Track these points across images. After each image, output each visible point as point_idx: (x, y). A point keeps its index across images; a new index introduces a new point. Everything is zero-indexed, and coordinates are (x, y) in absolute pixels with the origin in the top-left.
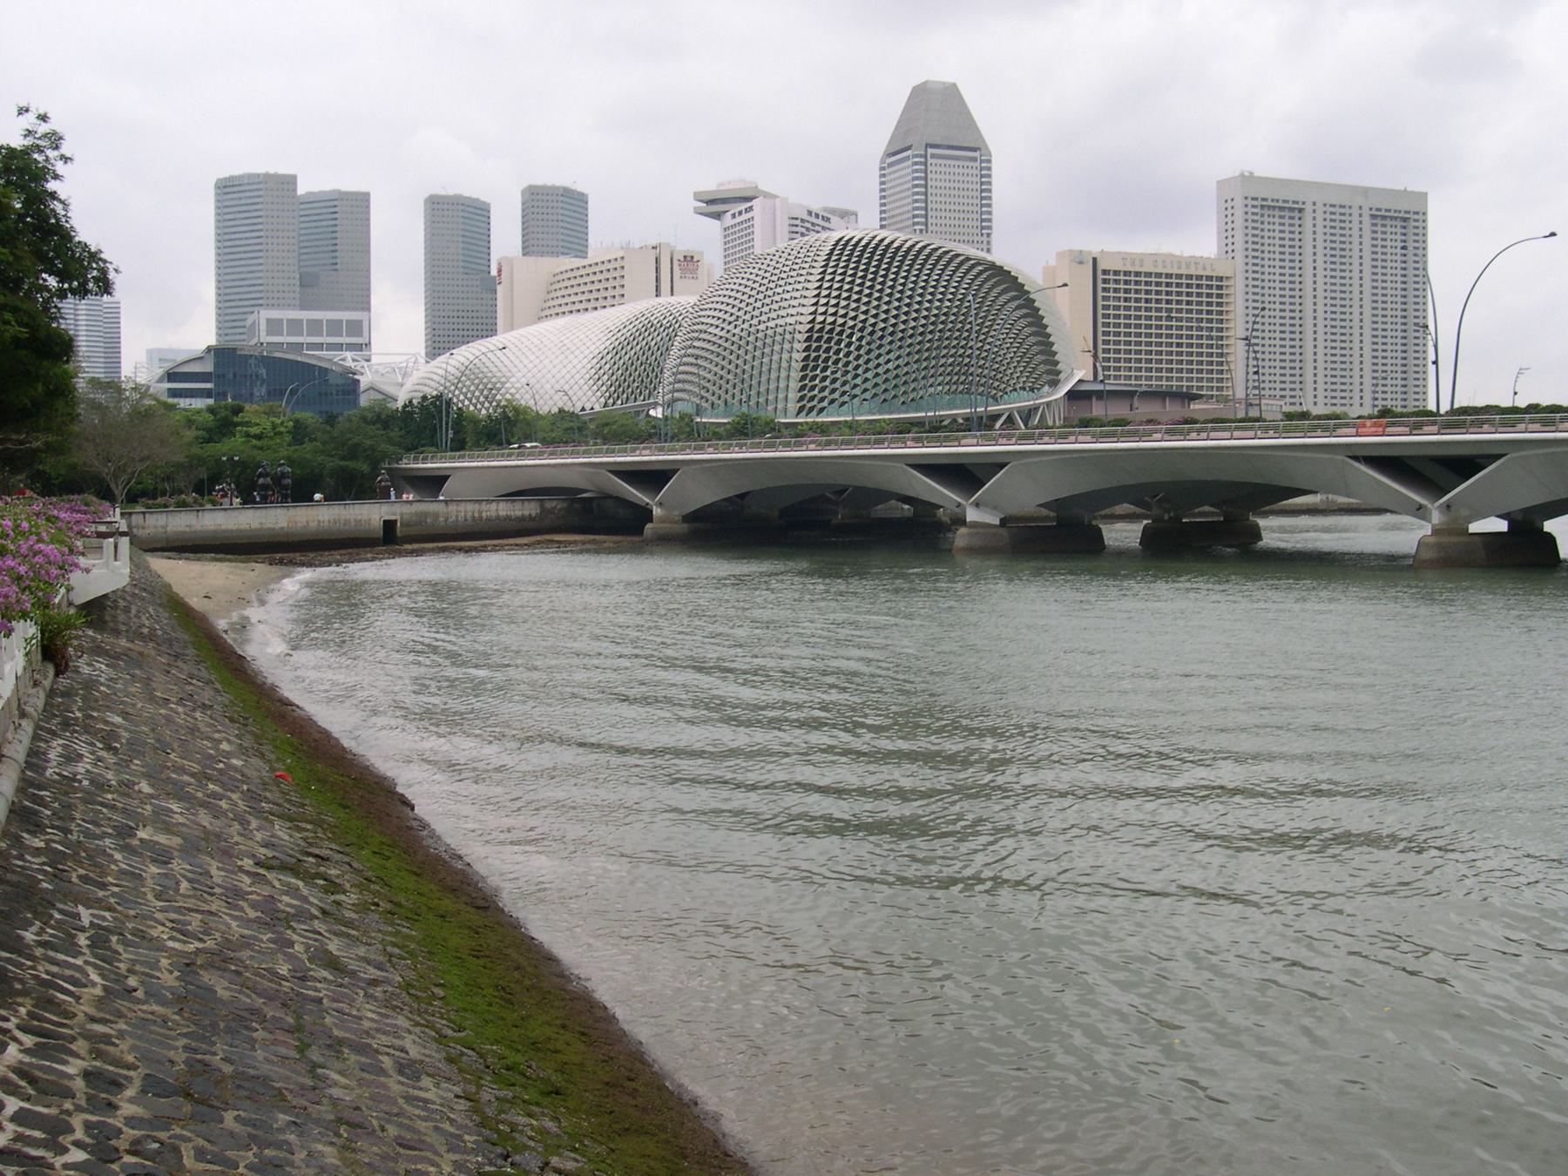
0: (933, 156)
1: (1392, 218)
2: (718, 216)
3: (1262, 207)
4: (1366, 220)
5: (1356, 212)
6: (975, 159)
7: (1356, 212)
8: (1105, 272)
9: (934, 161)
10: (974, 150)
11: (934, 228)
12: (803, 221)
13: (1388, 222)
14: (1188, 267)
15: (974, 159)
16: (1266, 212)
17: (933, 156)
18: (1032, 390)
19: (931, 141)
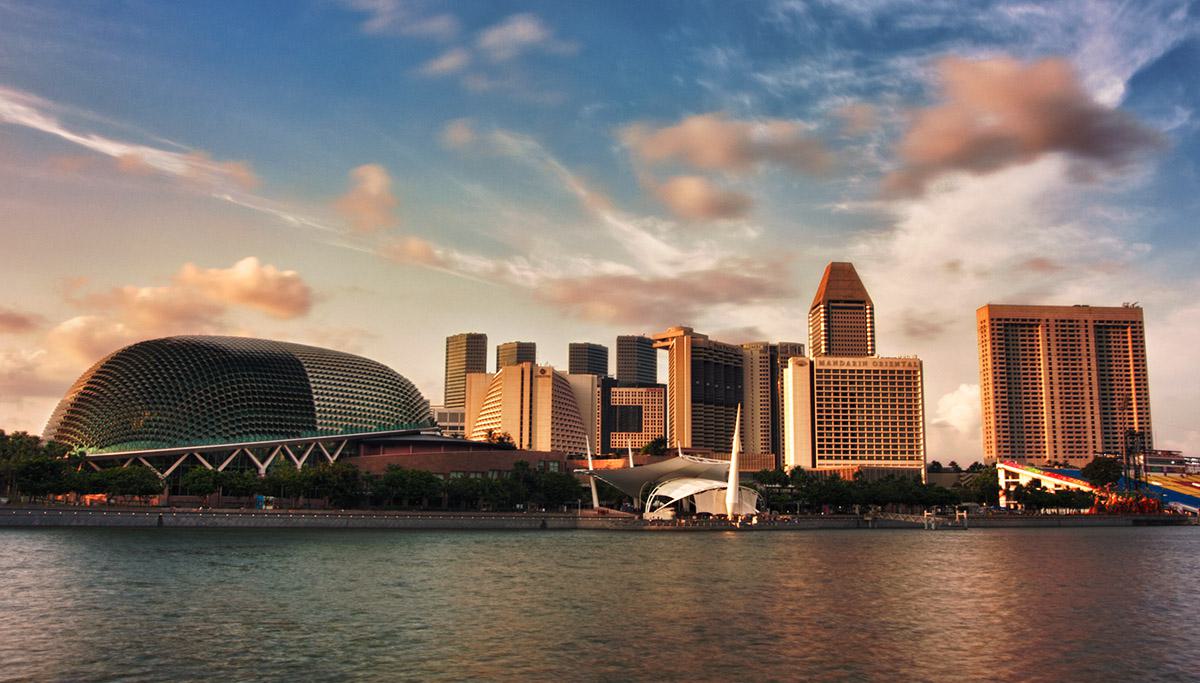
0: (833, 307)
1: (1114, 327)
2: (666, 348)
3: (1006, 325)
4: (1091, 329)
5: (1082, 324)
6: (862, 308)
7: (1082, 324)
8: (818, 371)
9: (834, 311)
10: (861, 302)
11: (835, 352)
12: (705, 349)
13: (1111, 330)
14: (891, 366)
15: (862, 308)
16: (1010, 328)
17: (833, 307)
18: (227, 438)
19: (832, 298)
